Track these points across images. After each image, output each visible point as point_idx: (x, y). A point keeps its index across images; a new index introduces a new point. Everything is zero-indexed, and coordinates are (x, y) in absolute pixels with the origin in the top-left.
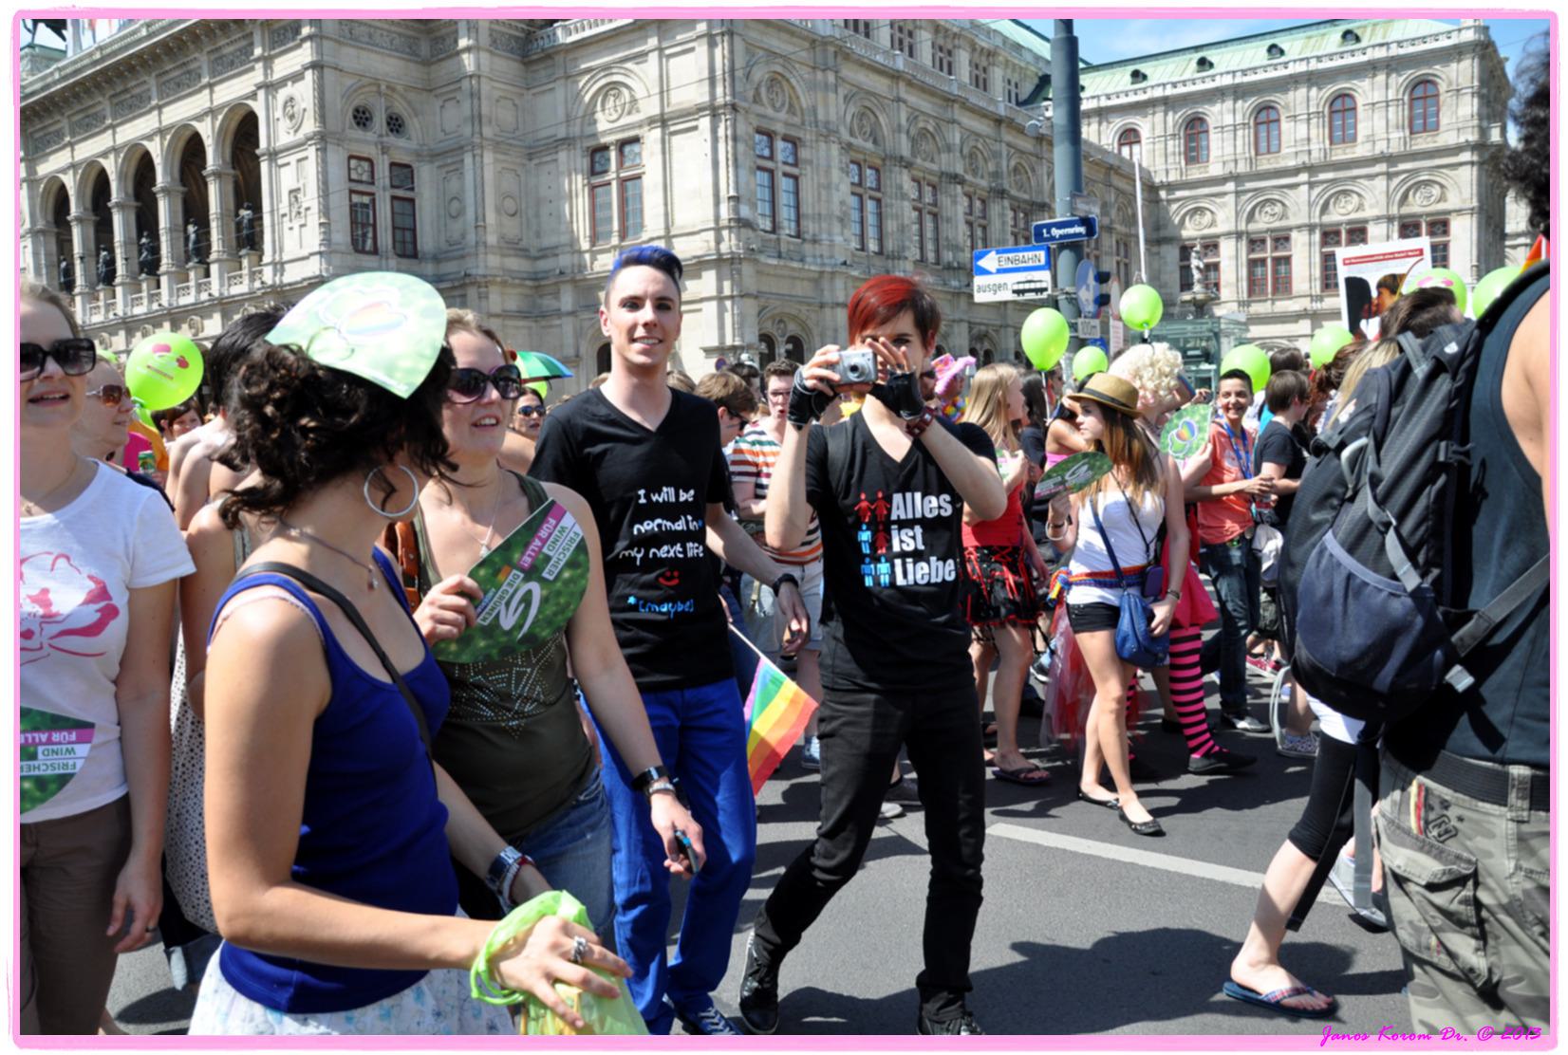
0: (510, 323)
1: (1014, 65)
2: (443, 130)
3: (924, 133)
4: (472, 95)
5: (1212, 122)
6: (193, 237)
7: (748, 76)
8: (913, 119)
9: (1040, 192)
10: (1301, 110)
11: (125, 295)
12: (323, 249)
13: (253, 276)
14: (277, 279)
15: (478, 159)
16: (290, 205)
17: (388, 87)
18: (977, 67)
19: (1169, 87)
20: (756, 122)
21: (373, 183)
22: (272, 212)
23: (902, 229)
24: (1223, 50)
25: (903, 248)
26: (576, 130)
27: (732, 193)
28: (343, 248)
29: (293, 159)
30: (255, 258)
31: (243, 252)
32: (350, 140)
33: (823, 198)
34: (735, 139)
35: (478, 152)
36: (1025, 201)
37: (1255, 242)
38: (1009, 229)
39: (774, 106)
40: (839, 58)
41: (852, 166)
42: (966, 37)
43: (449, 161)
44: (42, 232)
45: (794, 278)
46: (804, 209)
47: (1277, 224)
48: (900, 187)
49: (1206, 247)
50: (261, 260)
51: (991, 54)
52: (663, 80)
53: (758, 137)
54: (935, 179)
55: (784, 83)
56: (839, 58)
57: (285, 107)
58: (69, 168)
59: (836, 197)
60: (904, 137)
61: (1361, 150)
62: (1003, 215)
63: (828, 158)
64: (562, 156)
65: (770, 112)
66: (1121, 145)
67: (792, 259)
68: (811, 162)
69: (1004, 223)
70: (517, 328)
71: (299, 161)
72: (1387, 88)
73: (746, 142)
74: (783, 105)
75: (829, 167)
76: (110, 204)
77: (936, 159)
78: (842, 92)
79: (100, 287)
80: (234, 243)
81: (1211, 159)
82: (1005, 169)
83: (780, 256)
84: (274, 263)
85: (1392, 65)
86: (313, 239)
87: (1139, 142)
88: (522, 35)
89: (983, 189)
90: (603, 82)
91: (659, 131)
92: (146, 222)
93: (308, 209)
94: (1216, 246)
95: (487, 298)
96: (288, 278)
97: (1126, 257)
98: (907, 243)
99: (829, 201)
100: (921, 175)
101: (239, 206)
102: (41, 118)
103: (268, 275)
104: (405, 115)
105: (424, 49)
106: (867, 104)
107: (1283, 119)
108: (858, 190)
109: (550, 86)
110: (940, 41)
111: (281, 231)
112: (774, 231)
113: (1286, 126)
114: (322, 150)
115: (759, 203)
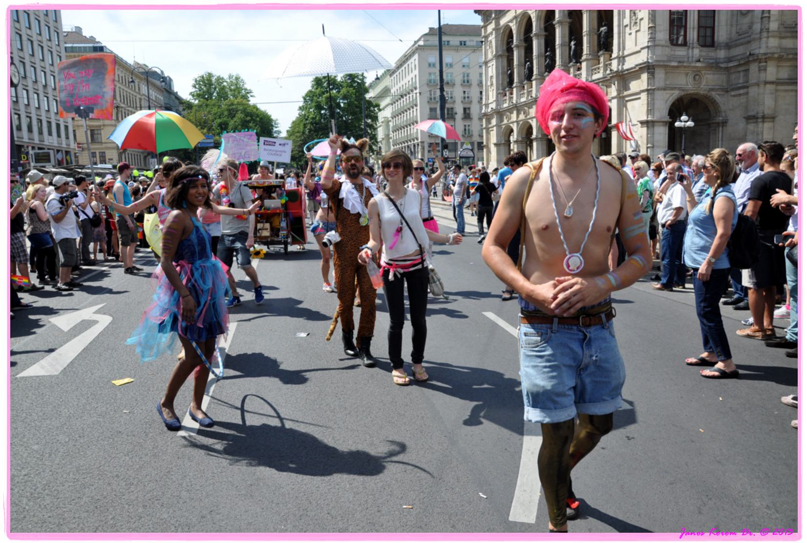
0: (780, 88)
6: (573, 47)
11: (536, 85)
12: (650, 44)
13: (606, 66)
14: (620, 67)
16: (631, 18)
22: (619, 26)
28: (663, 43)
30: (607, 56)
31: (601, 52)
44: (501, 56)
50: (611, 56)
58: (514, 19)
70: (786, 91)
76: (532, 35)
79: (526, 82)
80: (596, 49)
84: (618, 57)
86: (644, 38)
92: (549, 44)
93: (642, 19)
95: (765, 70)
96: (626, 67)
101: (600, 25)
103: (615, 65)
111: (624, 36)
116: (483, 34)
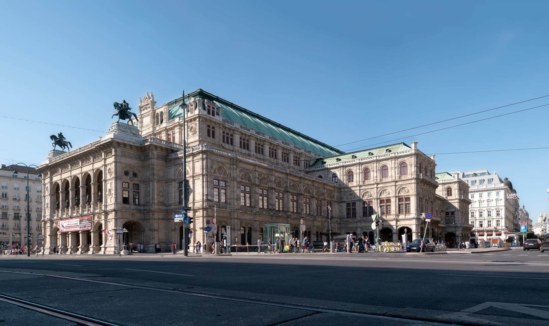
1: (308, 156)
2: (146, 176)
3: (264, 178)
4: (152, 169)
5: (354, 171)
7: (212, 168)
8: (260, 174)
9: (301, 191)
10: (375, 169)
15: (153, 184)
17: (133, 166)
18: (296, 157)
19: (344, 163)
20: (214, 177)
21: (128, 188)
23: (256, 201)
24: (360, 153)
25: (256, 205)
27: (206, 194)
29: (110, 182)
33: (232, 194)
34: (207, 182)
35: (153, 182)
36: (296, 193)
38: (290, 200)
39: (219, 174)
41: (241, 186)
42: (292, 151)
43: (147, 183)
45: (224, 212)
46: (227, 197)
48: (256, 191)
49: (353, 203)
51: (300, 154)
53: (215, 181)
54: (267, 189)
55: (222, 168)
56: (238, 162)
57: (108, 170)
59: (235, 194)
60: (257, 180)
61: (389, 179)
62: (288, 197)
63: (234, 185)
64: (173, 183)
65: (218, 175)
66: (333, 177)
67: (223, 208)
68: (229, 186)
69: (288, 199)
71: (111, 183)
72: (395, 164)
73: (210, 182)
74: (222, 173)
75: (234, 187)
77: (268, 184)
78: (238, 170)
81: (354, 181)
82: (289, 186)
83: (220, 208)
85: (396, 158)
88: (165, 155)
89: (282, 191)
91: (192, 179)
93: (112, 194)
94: (355, 203)
98: (257, 204)
99: (234, 195)
100: (263, 188)
102: (54, 168)
104: (137, 173)
105: (143, 158)
107: (371, 171)
108: (245, 192)
109: (171, 167)
110: (285, 151)
112: (219, 202)
113: (372, 173)
114: (116, 181)
115: (215, 196)
116: (43, 183)
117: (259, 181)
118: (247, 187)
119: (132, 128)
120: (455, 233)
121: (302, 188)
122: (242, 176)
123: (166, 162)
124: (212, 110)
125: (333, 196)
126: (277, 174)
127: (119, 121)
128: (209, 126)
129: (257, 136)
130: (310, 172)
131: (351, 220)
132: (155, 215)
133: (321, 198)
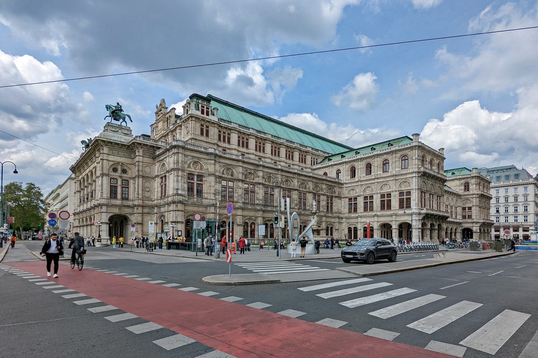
3: (250, 173)
26: (159, 174)
32: (111, 175)
37: (366, 198)
40: (217, 158)
47: (370, 193)
49: (354, 198)
52: (169, 163)
55: (198, 163)
68: (206, 181)
73: (182, 177)
77: (255, 179)
82: (280, 180)
87: (340, 173)
90: (162, 163)
97: (331, 201)
106: (229, 167)
117: (244, 176)
118: (230, 182)
119: (123, 128)
120: (472, 228)
121: (296, 183)
122: (223, 171)
123: (154, 158)
124: (206, 111)
125: (335, 191)
126: (266, 170)
127: (111, 121)
128: (202, 125)
129: (257, 135)
130: (316, 169)
131: (353, 215)
132: (139, 209)
133: (319, 194)
